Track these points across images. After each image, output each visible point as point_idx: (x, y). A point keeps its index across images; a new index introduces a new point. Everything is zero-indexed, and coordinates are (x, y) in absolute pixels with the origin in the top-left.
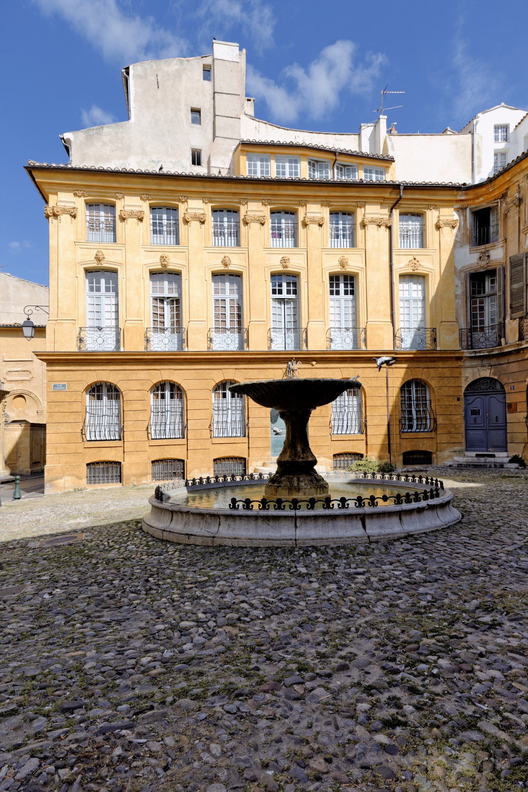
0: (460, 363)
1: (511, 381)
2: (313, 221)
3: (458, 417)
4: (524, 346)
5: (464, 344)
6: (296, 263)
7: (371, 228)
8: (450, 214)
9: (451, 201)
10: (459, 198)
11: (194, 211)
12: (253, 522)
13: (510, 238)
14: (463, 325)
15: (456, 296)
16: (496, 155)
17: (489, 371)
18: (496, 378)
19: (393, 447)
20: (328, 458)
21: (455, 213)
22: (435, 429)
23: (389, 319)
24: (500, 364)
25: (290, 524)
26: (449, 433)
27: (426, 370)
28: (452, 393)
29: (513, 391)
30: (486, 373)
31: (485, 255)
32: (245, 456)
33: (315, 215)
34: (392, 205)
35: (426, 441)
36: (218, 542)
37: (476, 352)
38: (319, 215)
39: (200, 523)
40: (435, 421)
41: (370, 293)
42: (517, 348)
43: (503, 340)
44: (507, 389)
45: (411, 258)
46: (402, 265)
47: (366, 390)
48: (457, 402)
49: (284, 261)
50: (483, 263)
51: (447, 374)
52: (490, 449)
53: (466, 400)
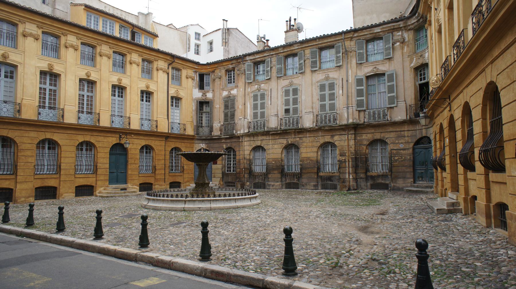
2: (135, 63)
6: (125, 82)
7: (160, 73)
8: (191, 73)
9: (192, 67)
11: (72, 42)
13: (216, 90)
14: (195, 124)
19: (166, 180)
22: (183, 171)
31: (204, 94)
32: (94, 185)
35: (179, 177)
40: (183, 167)
41: (159, 103)
45: (176, 90)
46: (172, 92)
47: (156, 151)
49: (120, 80)
50: (204, 98)
51: (189, 146)
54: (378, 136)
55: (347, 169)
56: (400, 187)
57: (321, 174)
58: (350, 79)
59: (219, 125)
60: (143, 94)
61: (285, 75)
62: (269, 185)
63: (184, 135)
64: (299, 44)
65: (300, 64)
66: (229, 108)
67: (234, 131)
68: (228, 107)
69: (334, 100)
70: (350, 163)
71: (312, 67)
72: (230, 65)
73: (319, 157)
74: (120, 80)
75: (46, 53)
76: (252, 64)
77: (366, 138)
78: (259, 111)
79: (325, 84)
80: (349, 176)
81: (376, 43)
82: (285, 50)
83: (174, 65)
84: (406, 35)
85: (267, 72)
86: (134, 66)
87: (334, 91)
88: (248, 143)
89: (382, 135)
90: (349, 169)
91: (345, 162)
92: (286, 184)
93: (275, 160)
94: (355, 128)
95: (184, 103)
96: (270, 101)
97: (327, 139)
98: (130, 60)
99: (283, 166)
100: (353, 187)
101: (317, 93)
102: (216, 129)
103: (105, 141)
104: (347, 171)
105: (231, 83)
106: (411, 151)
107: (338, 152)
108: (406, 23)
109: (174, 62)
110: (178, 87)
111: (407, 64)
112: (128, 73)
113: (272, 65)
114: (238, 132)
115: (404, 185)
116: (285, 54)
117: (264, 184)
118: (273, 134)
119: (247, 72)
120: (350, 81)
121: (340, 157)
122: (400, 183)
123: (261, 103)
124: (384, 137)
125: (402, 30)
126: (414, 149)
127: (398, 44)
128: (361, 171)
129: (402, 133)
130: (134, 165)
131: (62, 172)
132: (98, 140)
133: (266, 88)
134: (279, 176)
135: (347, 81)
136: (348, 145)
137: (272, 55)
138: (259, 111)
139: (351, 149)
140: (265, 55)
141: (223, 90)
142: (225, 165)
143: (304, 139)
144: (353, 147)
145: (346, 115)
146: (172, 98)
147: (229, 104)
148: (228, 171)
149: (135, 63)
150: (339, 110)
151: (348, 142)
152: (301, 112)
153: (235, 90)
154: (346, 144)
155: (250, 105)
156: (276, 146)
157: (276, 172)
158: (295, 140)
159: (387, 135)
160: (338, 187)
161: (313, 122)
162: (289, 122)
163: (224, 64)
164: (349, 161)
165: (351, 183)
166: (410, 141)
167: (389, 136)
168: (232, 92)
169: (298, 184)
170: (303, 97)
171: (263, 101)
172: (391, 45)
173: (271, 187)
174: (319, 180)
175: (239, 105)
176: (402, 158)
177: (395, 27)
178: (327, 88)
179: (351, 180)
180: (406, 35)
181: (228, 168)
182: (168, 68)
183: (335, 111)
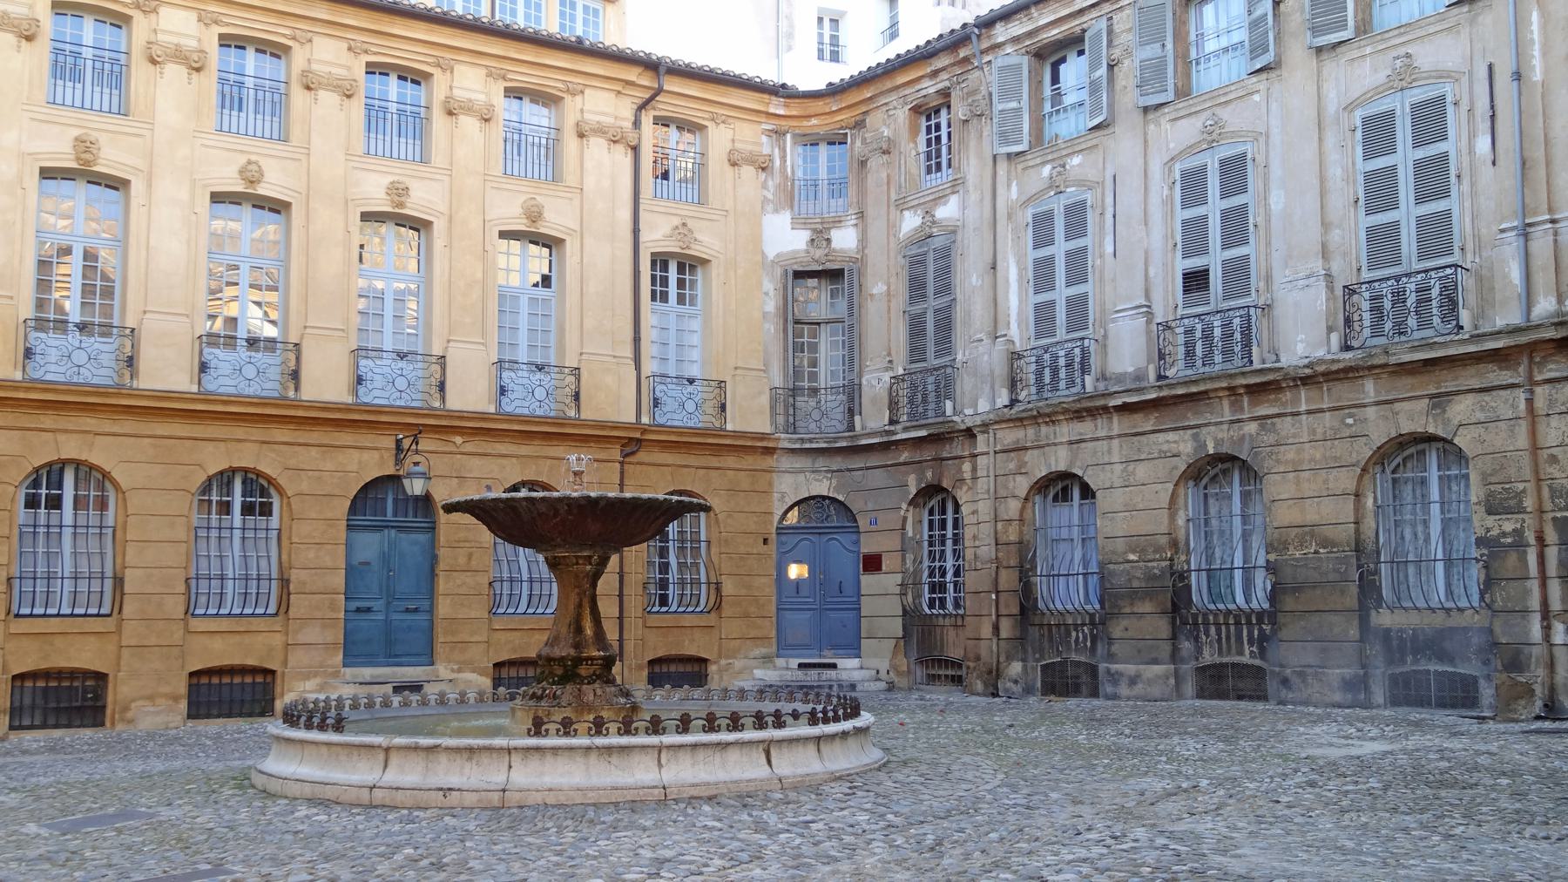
0: (770, 461)
1: (870, 506)
3: (764, 580)
4: (898, 437)
5: (781, 419)
7: (597, 146)
10: (772, 110)
11: (175, 40)
12: (580, 759)
13: (870, 212)
14: (778, 381)
15: (765, 315)
16: (820, 20)
17: (826, 483)
18: (841, 498)
20: (482, 672)
21: (764, 139)
22: (718, 606)
23: (628, 352)
24: (849, 470)
25: (649, 760)
26: (747, 616)
27: (702, 472)
28: (753, 528)
29: (873, 528)
30: (822, 487)
33: (473, 96)
34: (640, 102)
35: (697, 634)
36: (514, 798)
37: (802, 440)
38: (482, 97)
39: (462, 768)
40: (718, 590)
42: (885, 439)
43: (857, 418)
44: (863, 523)
45: (676, 221)
46: (657, 236)
48: (762, 548)
49: (398, 191)
50: (819, 253)
51: (745, 485)
53: (780, 544)
55: (1534, 586)
57: (1383, 619)
58: (1537, 62)
59: (886, 377)
60: (665, 268)
61: (1183, 92)
62: (1115, 678)
63: (721, 432)
65: (1255, 25)
66: (930, 290)
67: (949, 405)
68: (923, 286)
69: (1445, 194)
70: (1552, 554)
71: (1316, 30)
72: (926, 83)
73: (1369, 523)
74: (398, 191)
75: (69, 91)
78: (1061, 293)
80: (1547, 629)
83: (665, 106)
86: (469, 124)
87: (1440, 147)
91: (1520, 545)
92: (1201, 670)
93: (1138, 542)
95: (714, 286)
96: (1109, 240)
97: (1413, 418)
98: (448, 99)
99: (1183, 576)
101: (1347, 164)
103: (329, 466)
104: (1535, 603)
105: (939, 167)
109: (659, 91)
112: (438, 158)
113: (1117, 53)
117: (1093, 670)
118: (1125, 408)
120: (1538, 76)
121: (1490, 521)
123: (1069, 254)
130: (468, 579)
131: (128, 610)
132: (292, 463)
133: (1092, 174)
134: (1162, 627)
135: (1518, 76)
136: (1535, 448)
138: (1061, 293)
141: (902, 205)
142: (917, 573)
145: (1515, 274)
146: (660, 261)
147: (930, 271)
148: (931, 605)
149: (469, 108)
150: (1479, 248)
151: (1533, 433)
152: (1269, 279)
153: (954, 201)
154: (1522, 441)
155: (1022, 270)
156: (1142, 471)
157: (1147, 607)
158: (1235, 432)
160: (1487, 693)
161: (1330, 329)
162: (1207, 336)
163: (901, 79)
164: (1541, 539)
169: (1258, 672)
171: (1079, 243)
173: (1124, 690)
174: (1375, 650)
175: (969, 278)
178: (1404, 131)
182: (637, 124)
183: (1455, 258)
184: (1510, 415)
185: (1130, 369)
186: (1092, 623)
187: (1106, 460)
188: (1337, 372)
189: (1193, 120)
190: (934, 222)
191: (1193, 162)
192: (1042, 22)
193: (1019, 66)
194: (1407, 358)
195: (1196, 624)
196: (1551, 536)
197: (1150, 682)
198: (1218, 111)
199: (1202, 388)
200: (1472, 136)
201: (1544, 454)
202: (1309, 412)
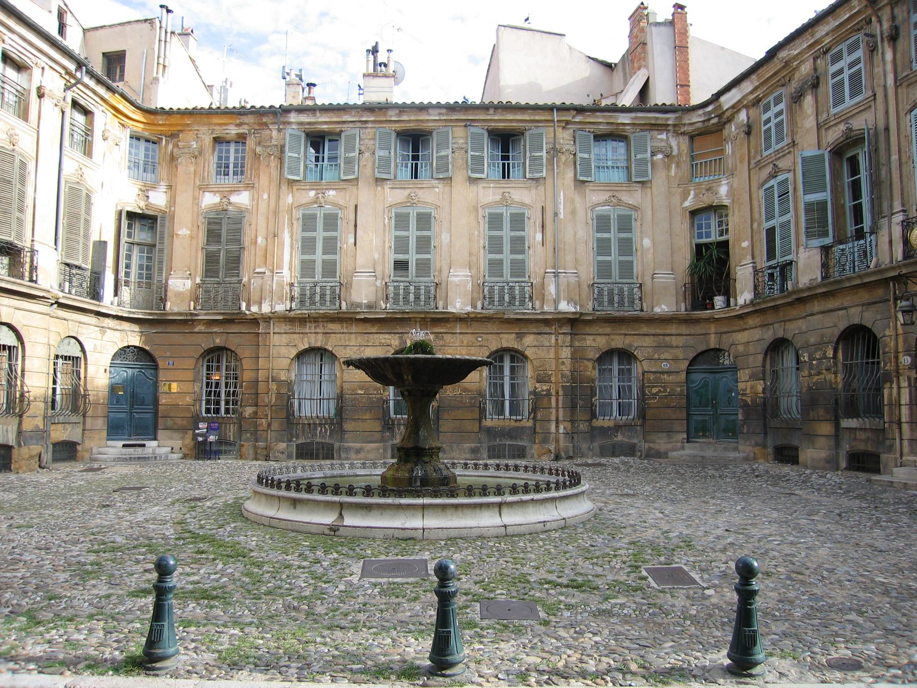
4: (200, 318)
13: (180, 187)
30: (135, 340)
42: (189, 318)
44: (161, 364)
52: (133, 437)
53: (110, 372)
54: (618, 342)
55: (554, 411)
56: (662, 451)
59: (189, 284)
62: (347, 450)
64: (444, 111)
66: (223, 239)
67: (244, 306)
68: (220, 236)
70: (561, 398)
72: (232, 127)
76: (303, 135)
77: (594, 344)
79: (502, 215)
80: (557, 427)
81: (611, 144)
82: (405, 118)
84: (674, 143)
85: (348, 161)
88: (284, 339)
89: (627, 341)
90: (556, 409)
91: (549, 394)
94: (575, 323)
100: (567, 452)
101: (482, 233)
102: (179, 294)
104: (553, 417)
106: (683, 376)
107: (529, 371)
108: (680, 118)
110: (84, 159)
111: (676, 199)
113: (363, 148)
114: (254, 309)
115: (669, 446)
116: (398, 127)
119: (288, 154)
120: (562, 216)
121: (538, 385)
122: (661, 443)
124: (631, 345)
125: (668, 131)
126: (688, 373)
127: (660, 156)
128: (581, 415)
129: (667, 338)
133: (341, 202)
134: (377, 426)
135: (556, 214)
136: (557, 358)
137: (366, 122)
139: (563, 368)
140: (347, 118)
141: (204, 188)
143: (448, 338)
144: (568, 362)
148: (208, 411)
151: (556, 352)
152: (440, 271)
154: (552, 355)
159: (637, 342)
163: (216, 120)
164: (557, 393)
165: (562, 444)
166: (681, 357)
167: (640, 343)
168: (234, 199)
170: (445, 238)
172: (649, 155)
173: (353, 455)
176: (665, 391)
177: (659, 122)
179: (562, 437)
180: (674, 143)
181: (208, 402)
184: (548, 344)
185: (365, 301)
186: (332, 424)
187: (347, 343)
188: (481, 318)
189: (402, 191)
190: (230, 203)
191: (404, 211)
192: (321, 120)
193: (300, 137)
194: (512, 316)
195: (393, 424)
196: (561, 393)
197: (368, 452)
198: (417, 191)
199: (410, 316)
200: (535, 232)
201: (560, 361)
202: (461, 333)
